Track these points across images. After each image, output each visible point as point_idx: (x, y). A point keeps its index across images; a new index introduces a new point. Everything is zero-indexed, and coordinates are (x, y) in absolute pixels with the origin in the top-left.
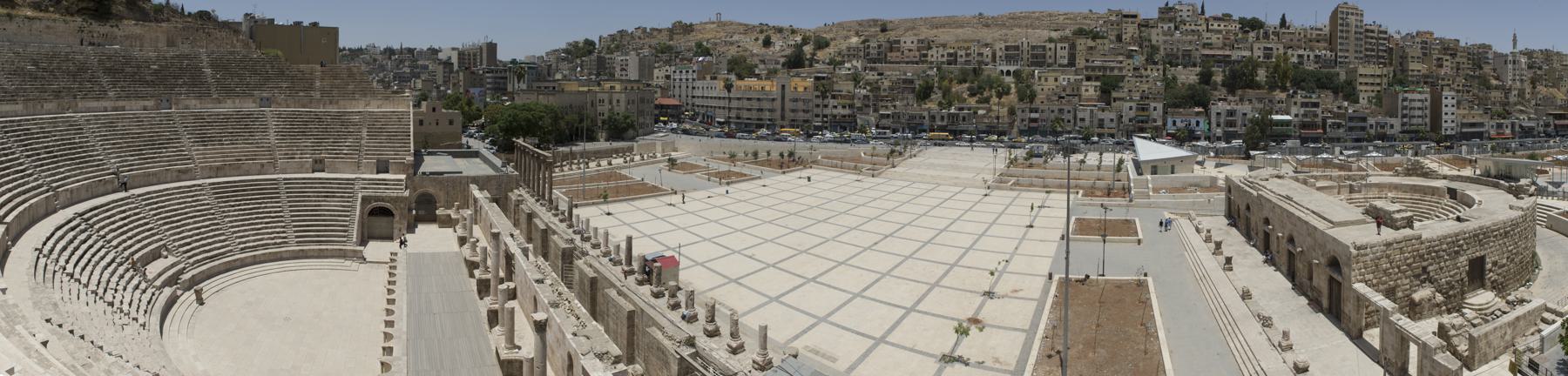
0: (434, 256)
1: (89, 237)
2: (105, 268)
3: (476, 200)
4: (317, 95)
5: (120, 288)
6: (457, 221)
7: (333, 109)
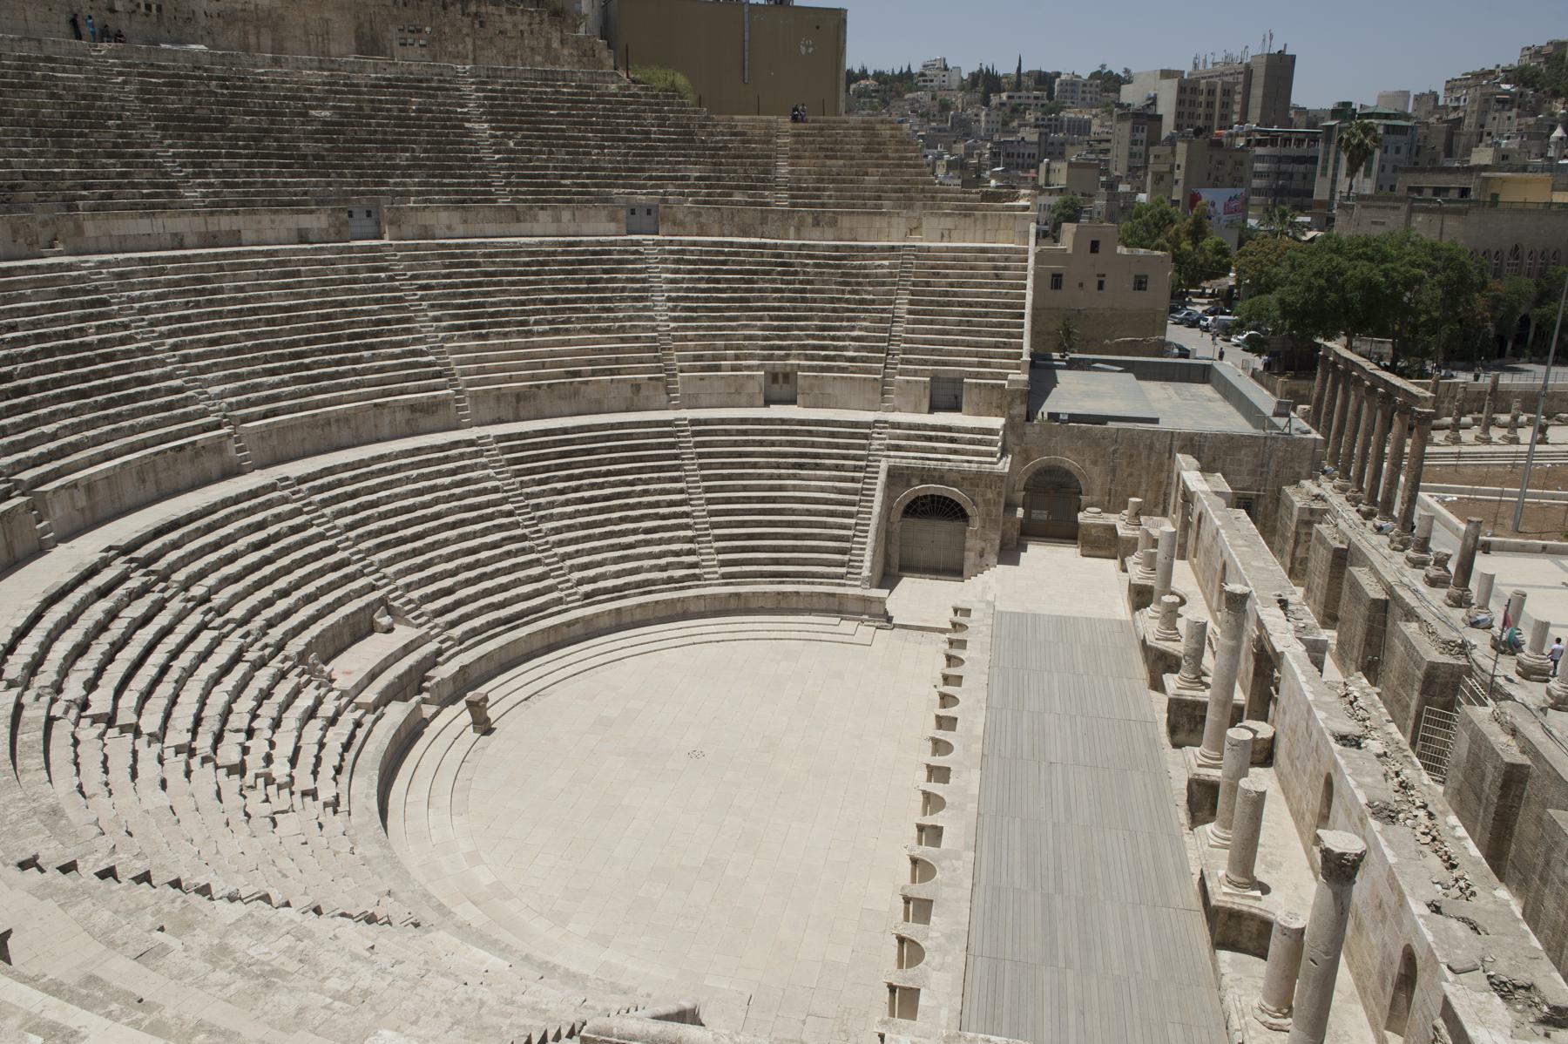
0: (1061, 622)
1: (160, 606)
2: (216, 680)
3: (1188, 497)
4: (781, 200)
5: (263, 724)
6: (1131, 546)
7: (823, 240)
